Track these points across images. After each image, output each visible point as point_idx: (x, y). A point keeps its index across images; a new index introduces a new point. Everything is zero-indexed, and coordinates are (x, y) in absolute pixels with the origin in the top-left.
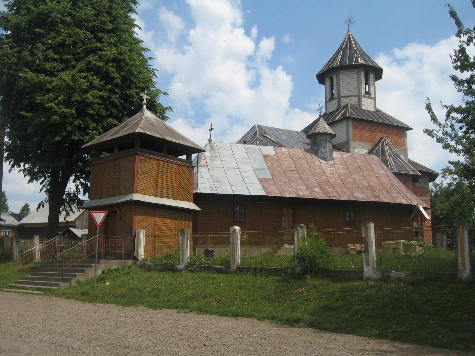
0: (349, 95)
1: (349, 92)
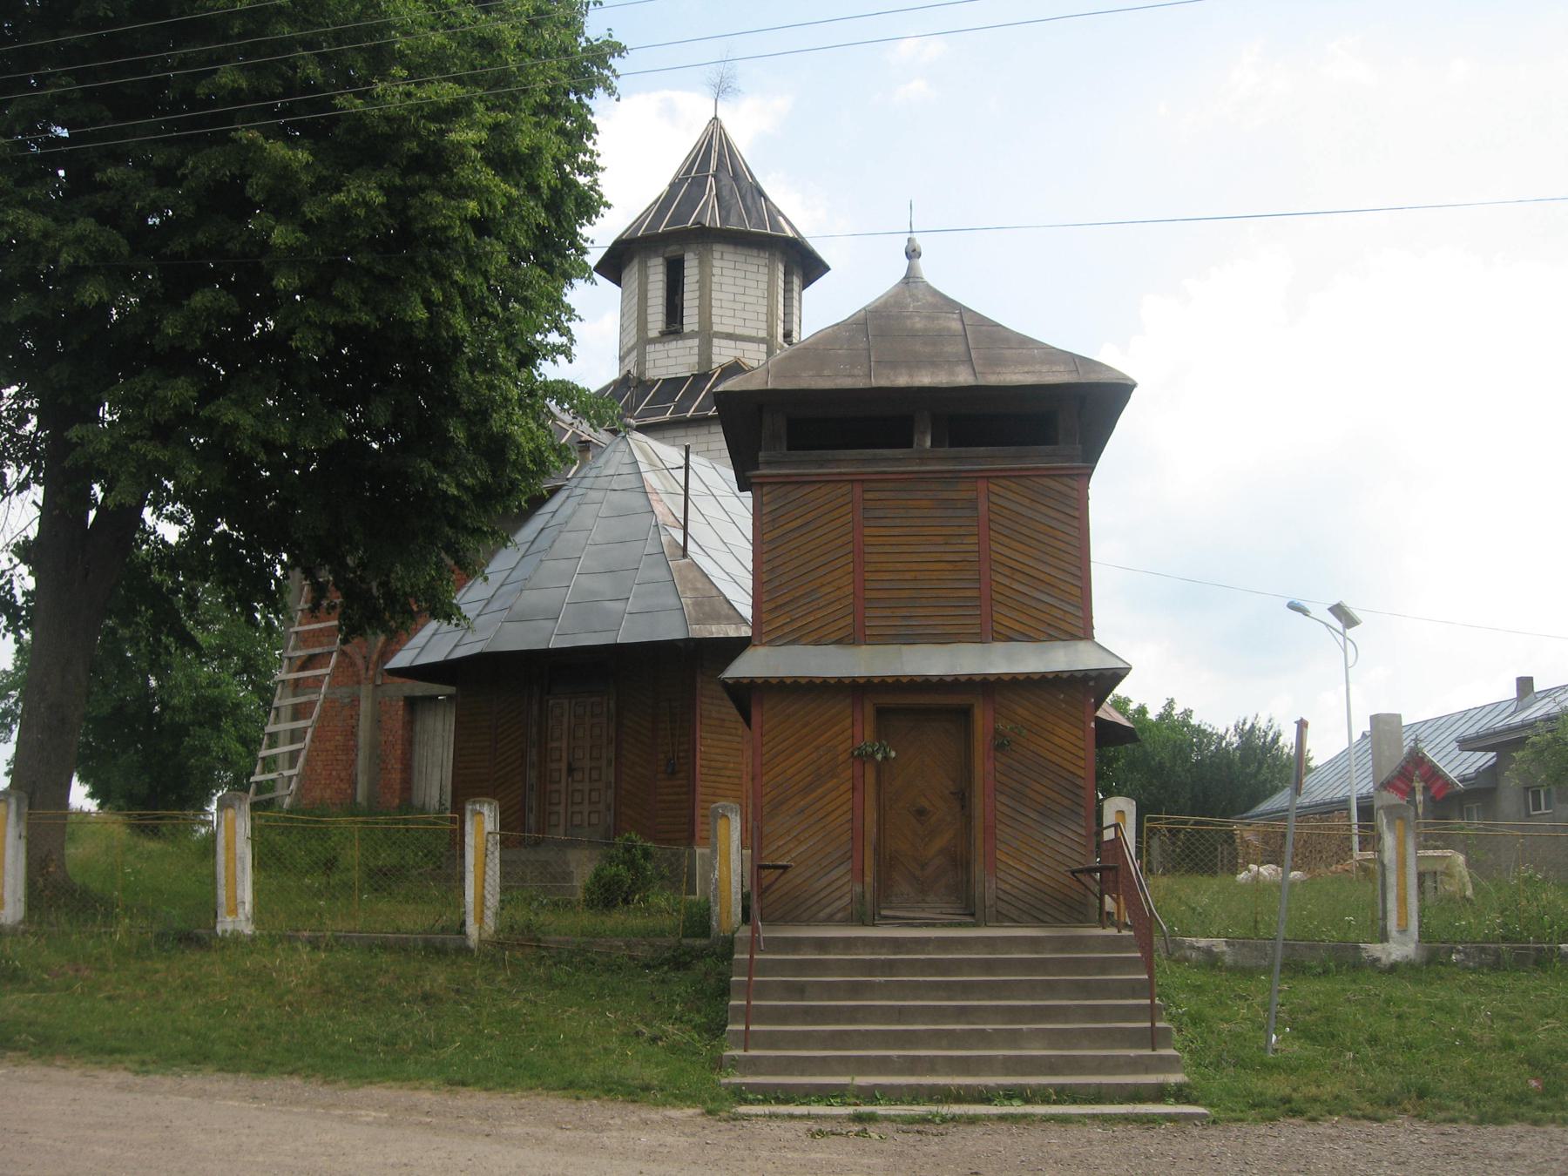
0: (738, 331)
1: (741, 322)
